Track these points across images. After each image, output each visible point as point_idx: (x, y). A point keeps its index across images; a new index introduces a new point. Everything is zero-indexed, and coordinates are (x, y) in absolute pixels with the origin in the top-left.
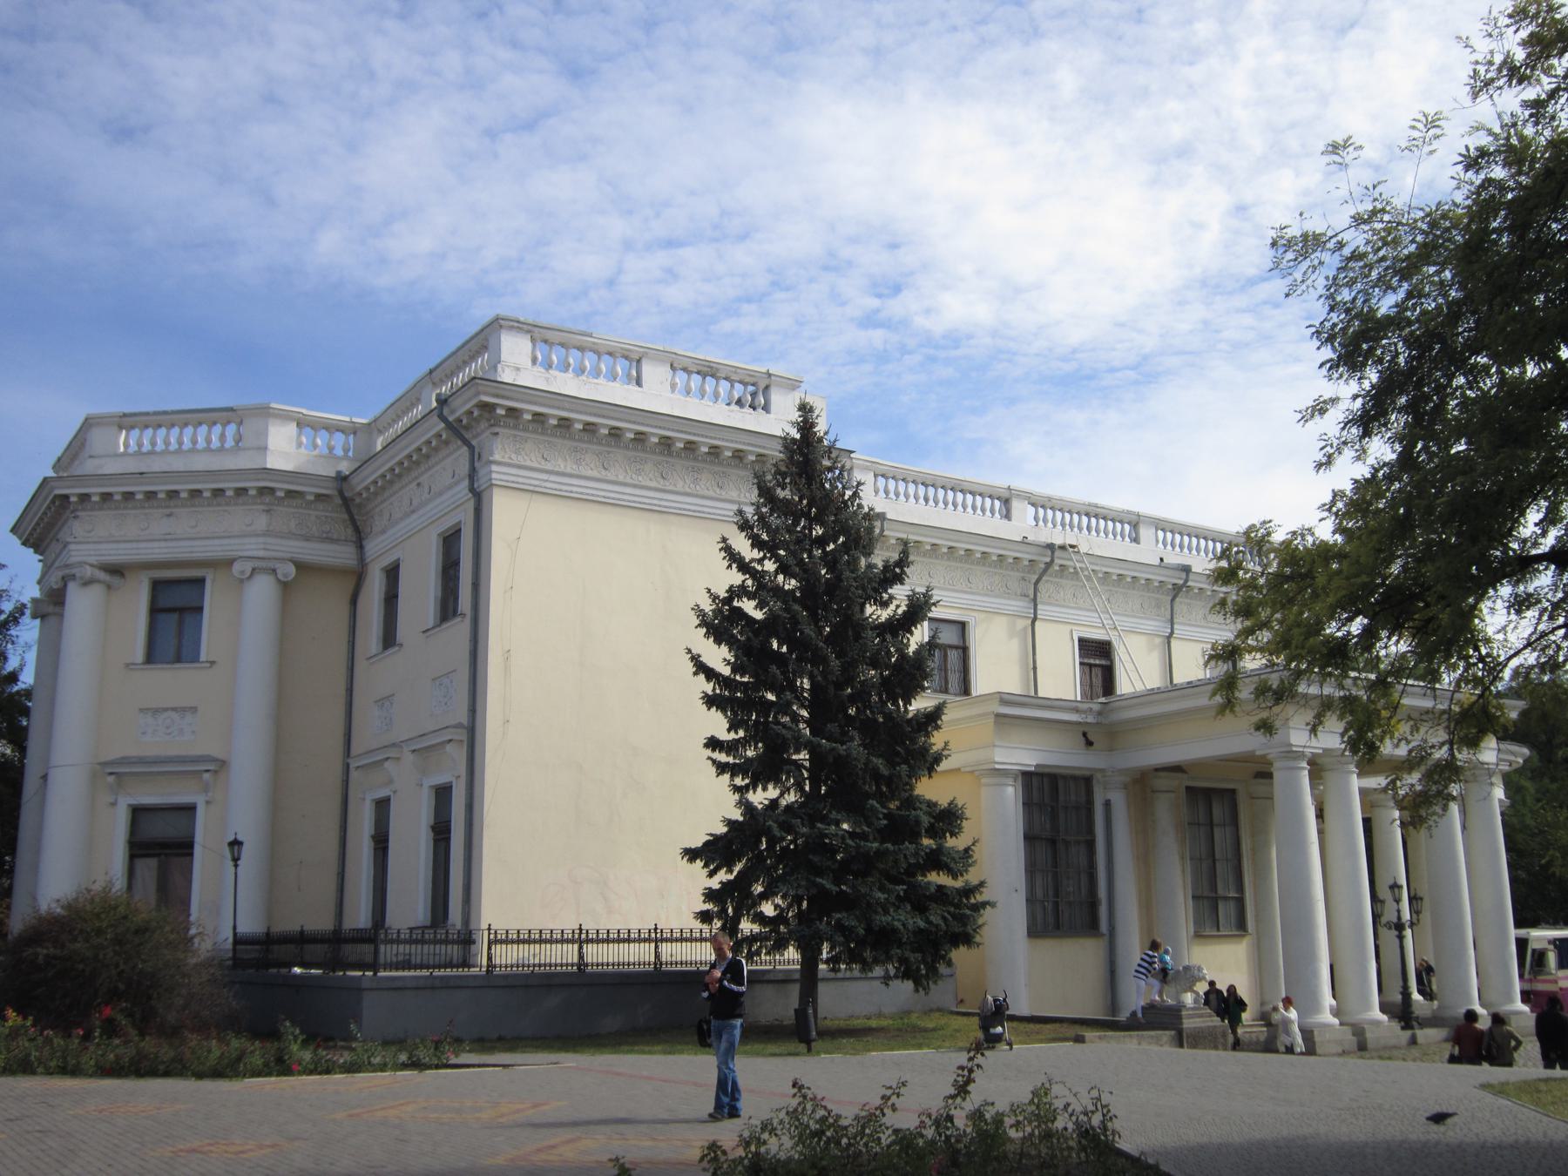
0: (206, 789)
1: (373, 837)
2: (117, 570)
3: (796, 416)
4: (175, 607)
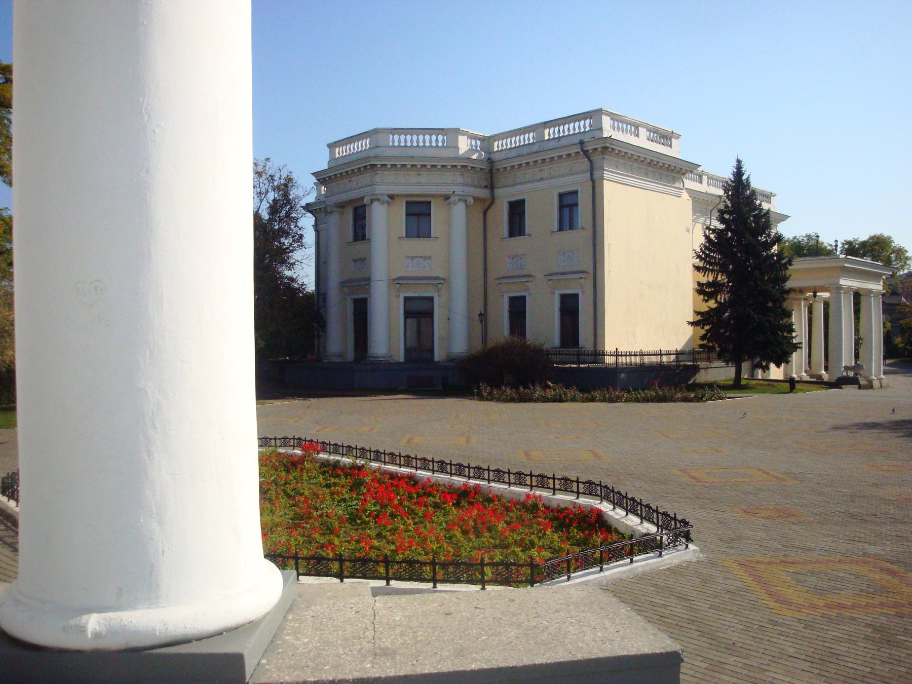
0: (439, 290)
1: (509, 311)
2: (392, 197)
3: (735, 164)
4: (418, 213)
